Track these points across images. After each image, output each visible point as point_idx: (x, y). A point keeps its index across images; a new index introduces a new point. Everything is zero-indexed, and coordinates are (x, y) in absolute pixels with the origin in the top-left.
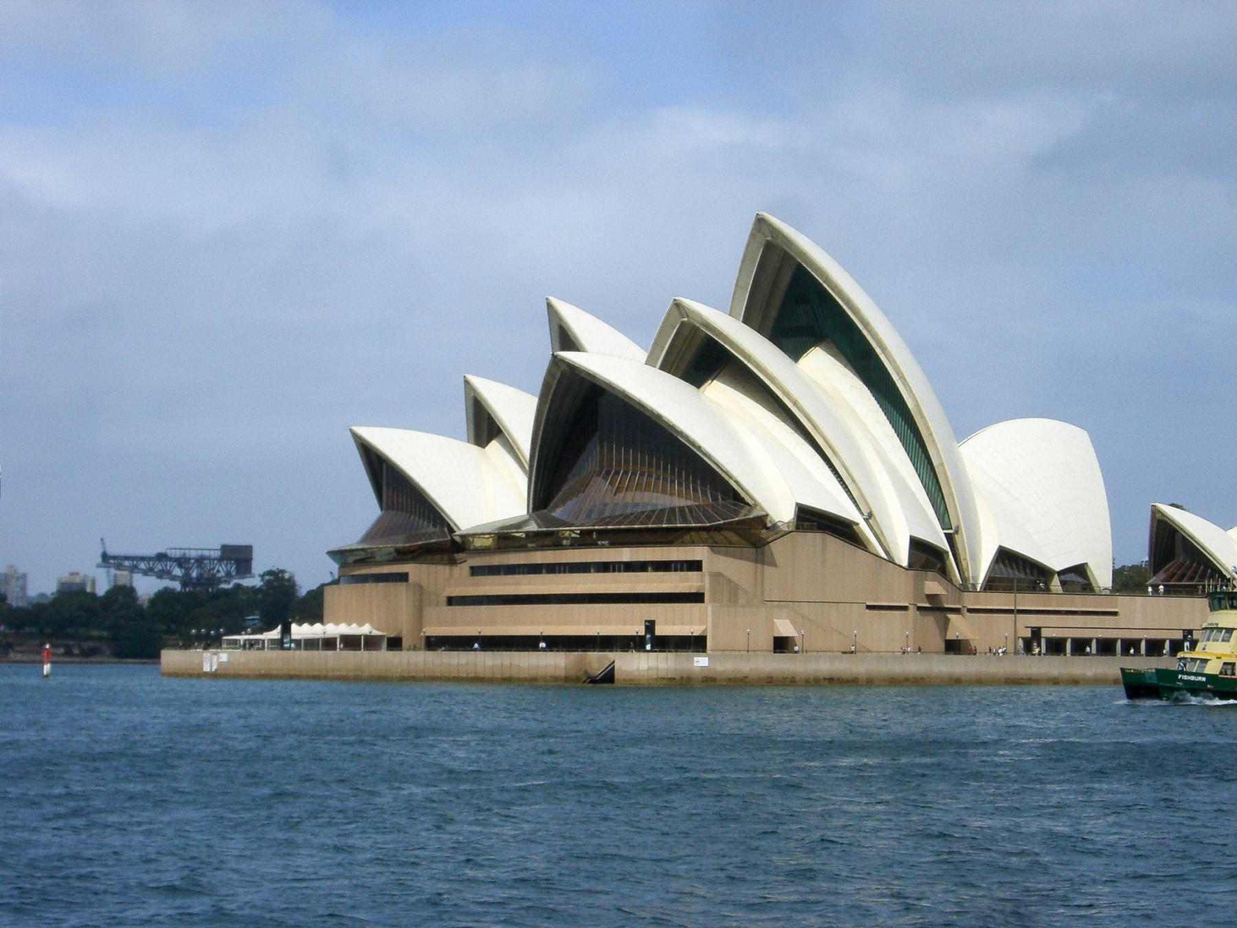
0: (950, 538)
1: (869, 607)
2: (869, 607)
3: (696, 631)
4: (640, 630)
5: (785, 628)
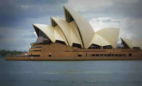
0: (83, 43)
1: (65, 51)
2: (65, 51)
3: (38, 54)
4: (31, 54)
5: (50, 54)
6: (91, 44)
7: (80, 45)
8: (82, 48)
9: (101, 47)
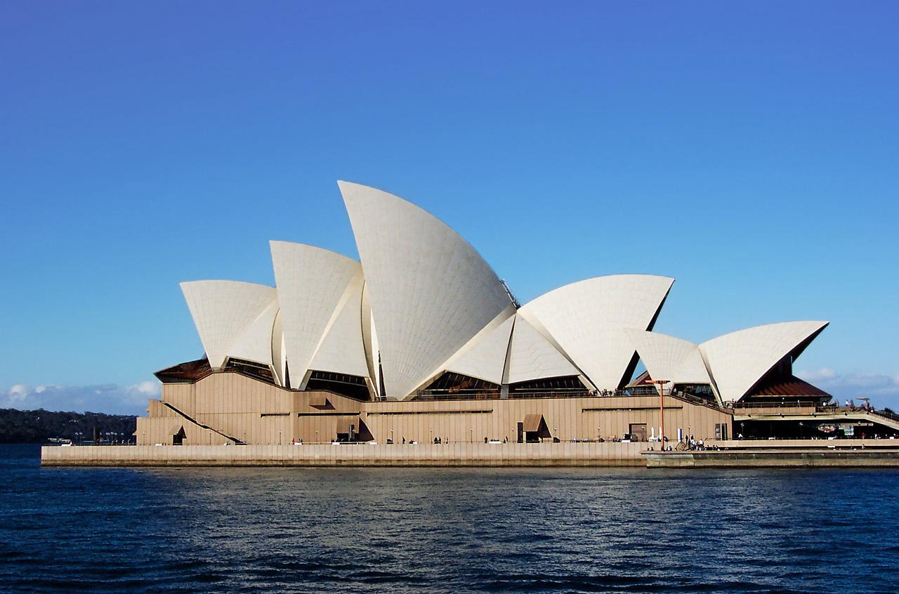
0: (380, 366)
1: (262, 415)
2: (262, 415)
6: (436, 372)
7: (361, 379)
8: (373, 398)
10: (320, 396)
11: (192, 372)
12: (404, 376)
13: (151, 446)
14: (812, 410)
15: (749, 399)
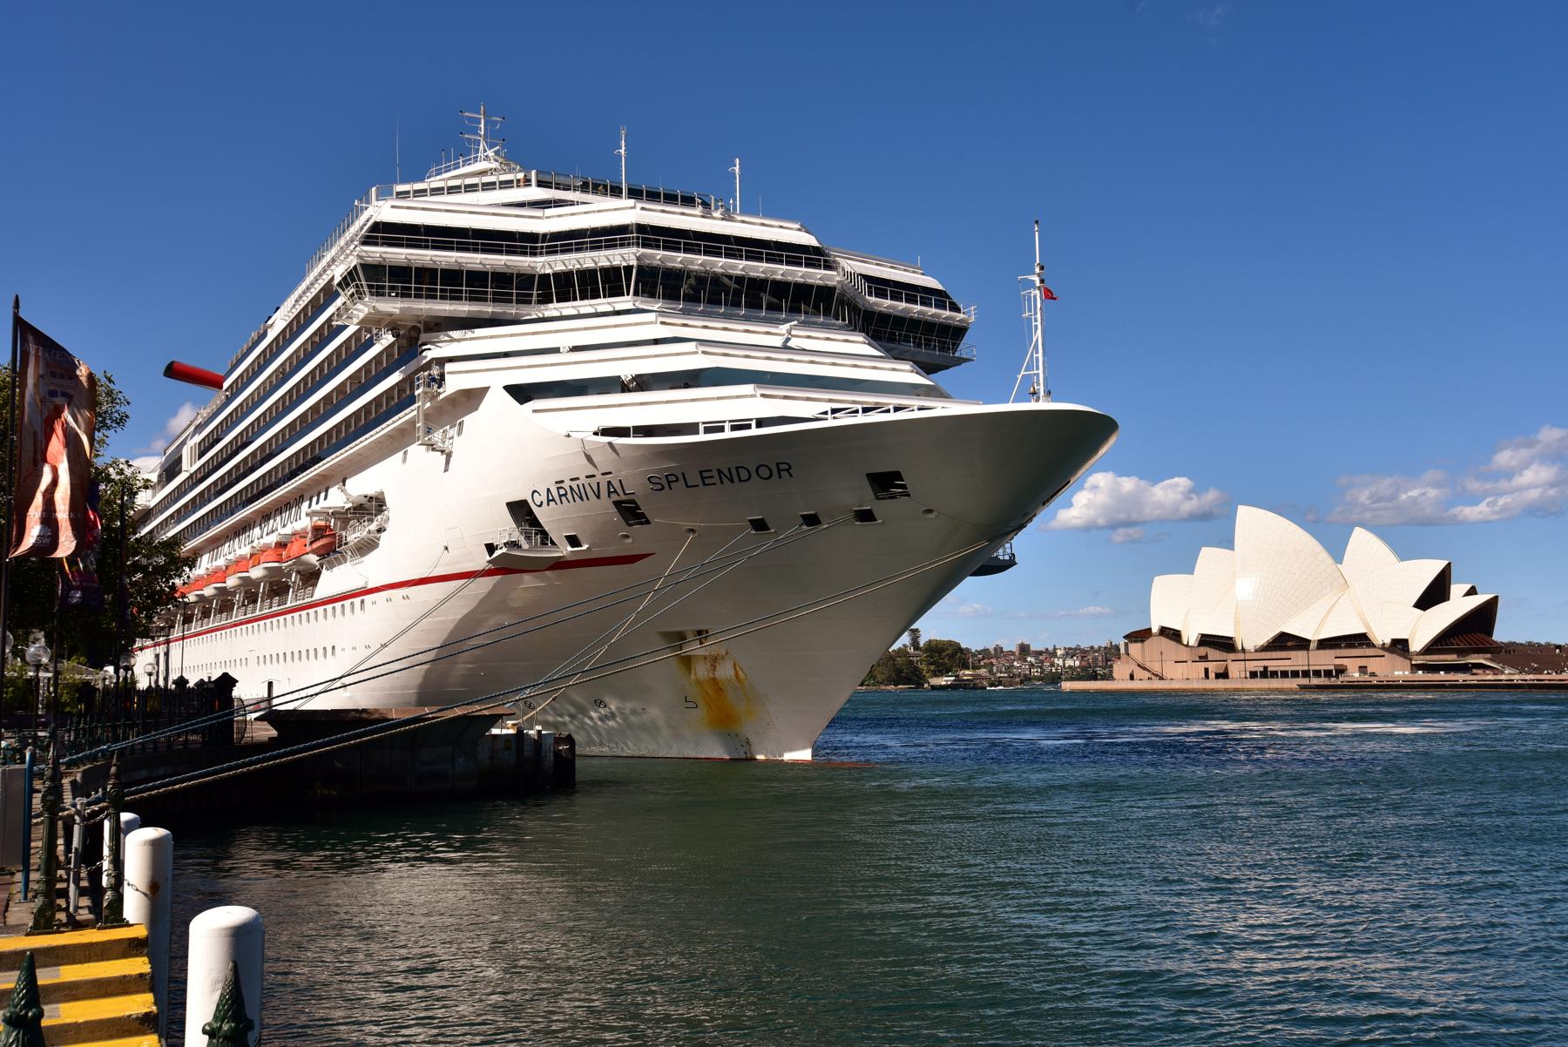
6: (1277, 632)
9: (1309, 641)
10: (1203, 651)
11: (1141, 636)
12: (1252, 637)
13: (1121, 679)
14: (1454, 657)
15: (1428, 650)
